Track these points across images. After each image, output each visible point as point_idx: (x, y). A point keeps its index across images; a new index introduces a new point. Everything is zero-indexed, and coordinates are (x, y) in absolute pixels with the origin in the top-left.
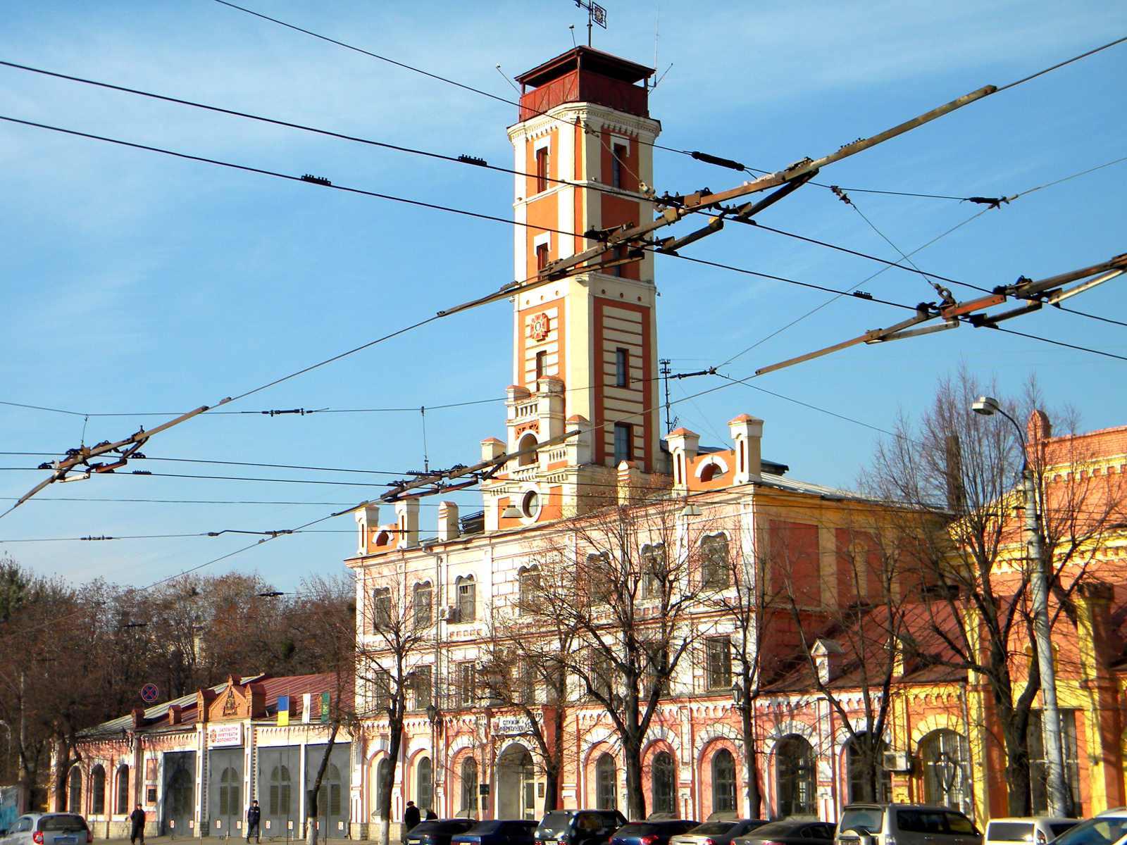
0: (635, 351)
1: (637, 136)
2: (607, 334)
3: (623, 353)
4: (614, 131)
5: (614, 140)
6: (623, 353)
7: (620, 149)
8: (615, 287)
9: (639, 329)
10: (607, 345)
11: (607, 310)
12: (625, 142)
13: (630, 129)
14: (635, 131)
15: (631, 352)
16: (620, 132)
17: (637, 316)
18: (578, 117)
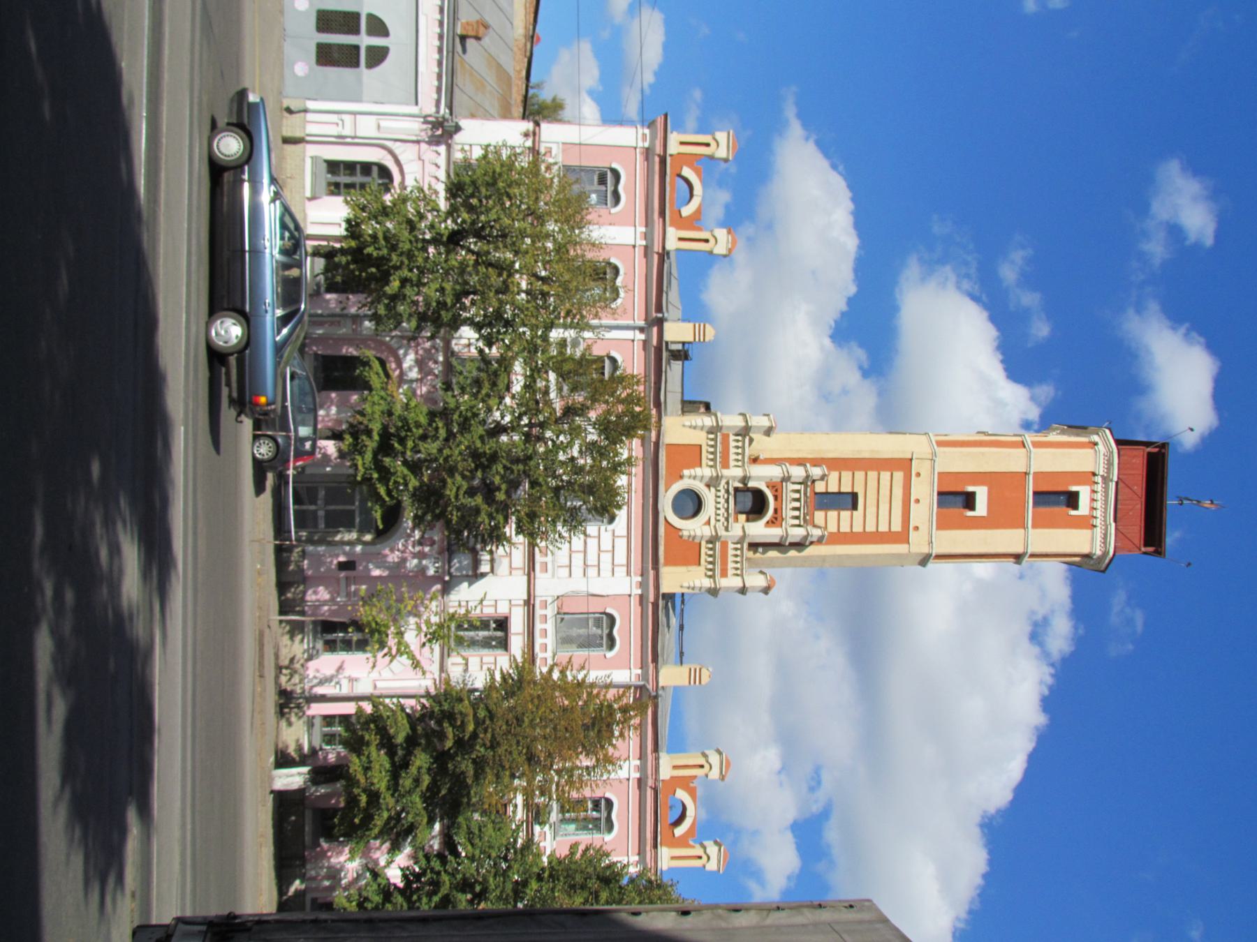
0: (858, 514)
1: (1095, 526)
2: (872, 475)
3: (852, 501)
4: (1094, 492)
5: (1084, 492)
6: (852, 501)
7: (1072, 500)
8: (925, 491)
9: (883, 528)
10: (860, 475)
11: (899, 476)
12: (1083, 508)
13: (1098, 513)
14: (1098, 522)
15: (855, 512)
16: (1093, 500)
17: (897, 527)
18: (1096, 444)
